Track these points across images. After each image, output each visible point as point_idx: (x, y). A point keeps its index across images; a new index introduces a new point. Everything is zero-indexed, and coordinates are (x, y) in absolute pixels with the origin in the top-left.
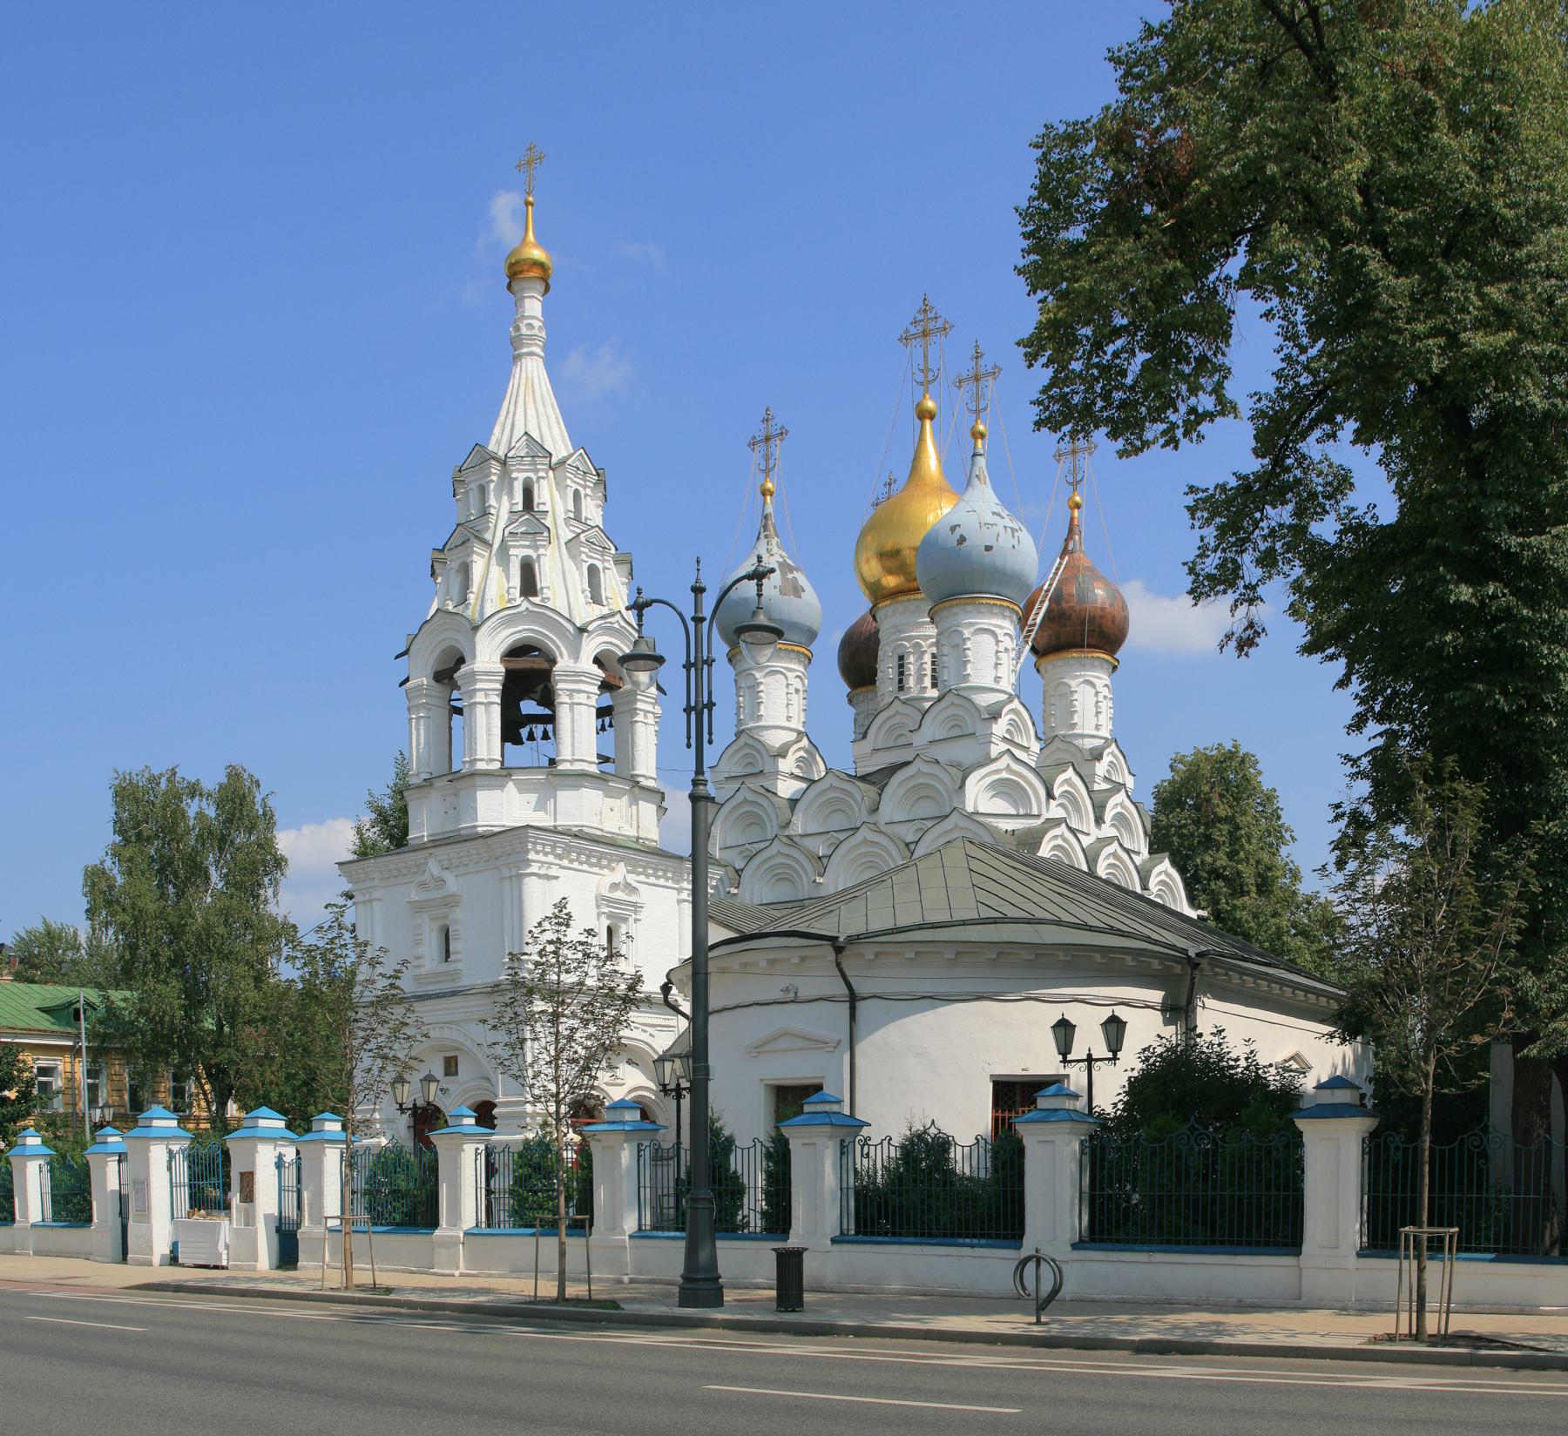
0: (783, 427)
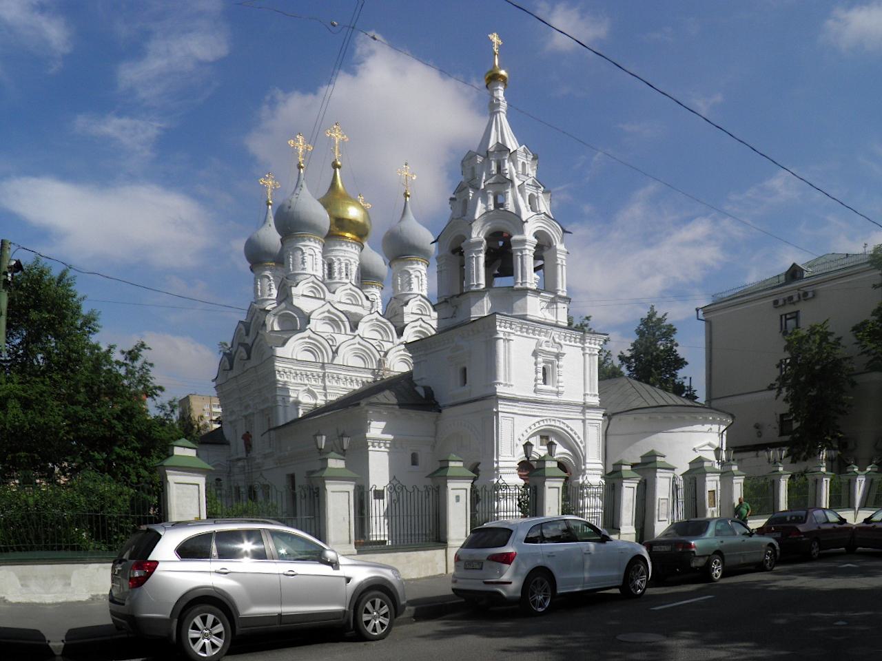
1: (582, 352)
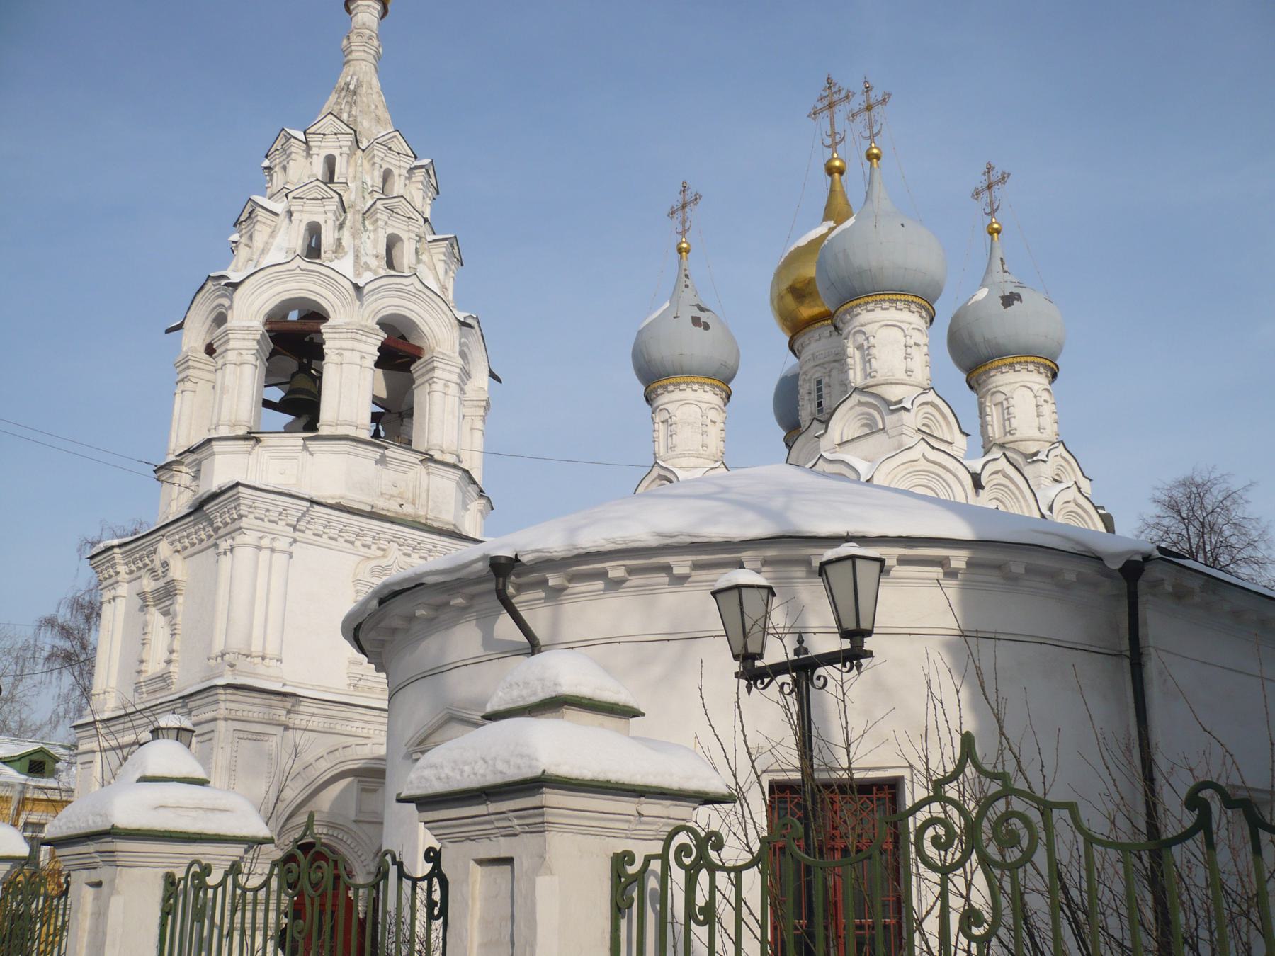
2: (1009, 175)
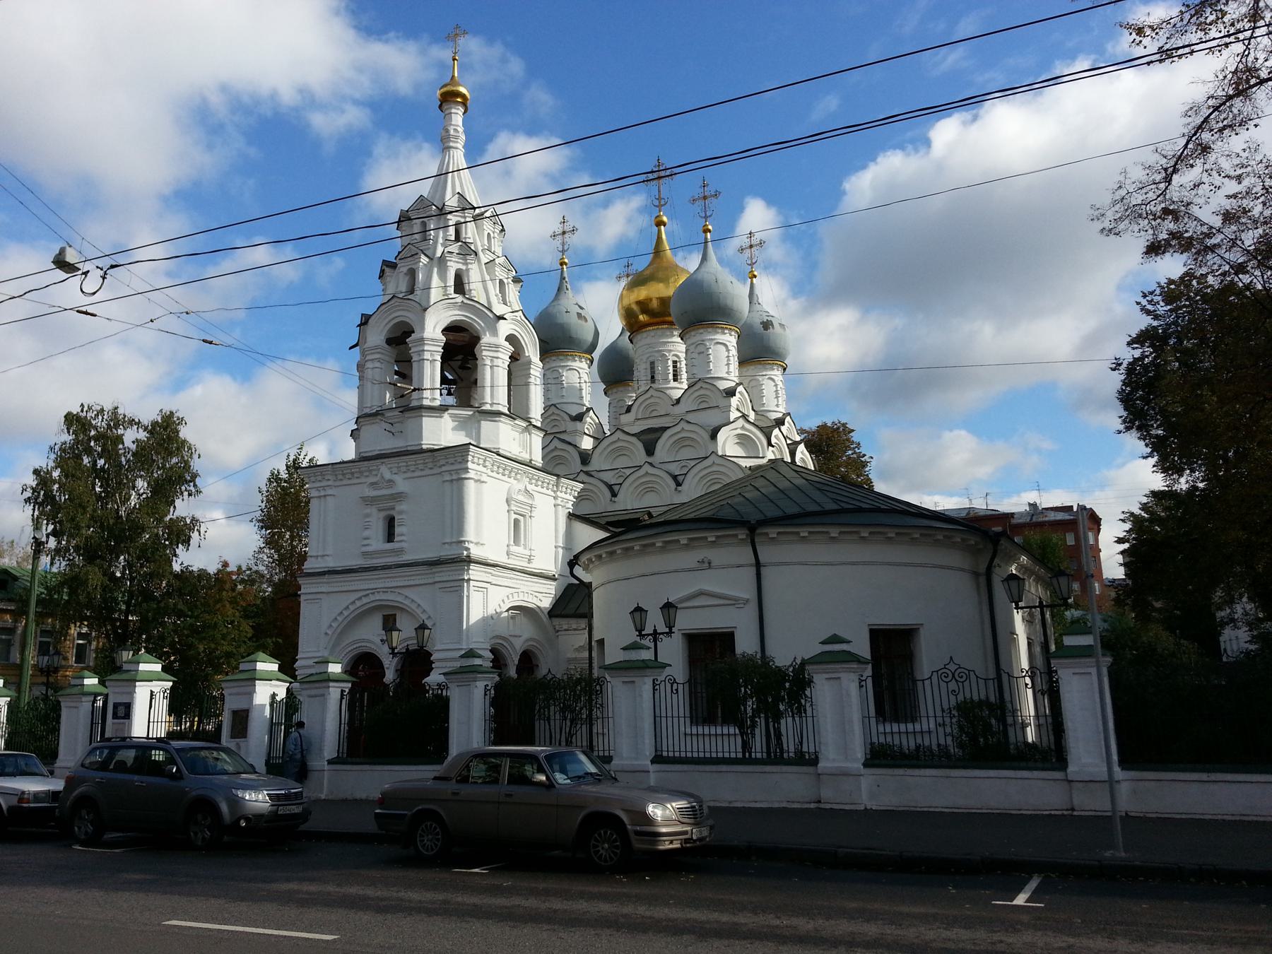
0: (574, 227)
1: (553, 501)
2: (764, 242)
